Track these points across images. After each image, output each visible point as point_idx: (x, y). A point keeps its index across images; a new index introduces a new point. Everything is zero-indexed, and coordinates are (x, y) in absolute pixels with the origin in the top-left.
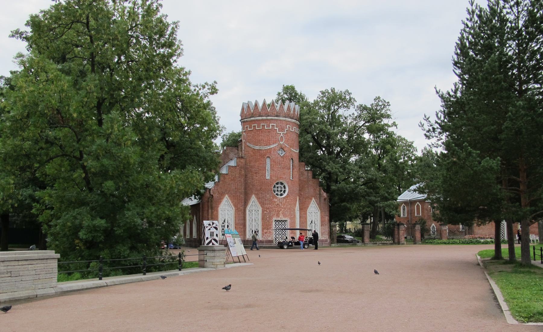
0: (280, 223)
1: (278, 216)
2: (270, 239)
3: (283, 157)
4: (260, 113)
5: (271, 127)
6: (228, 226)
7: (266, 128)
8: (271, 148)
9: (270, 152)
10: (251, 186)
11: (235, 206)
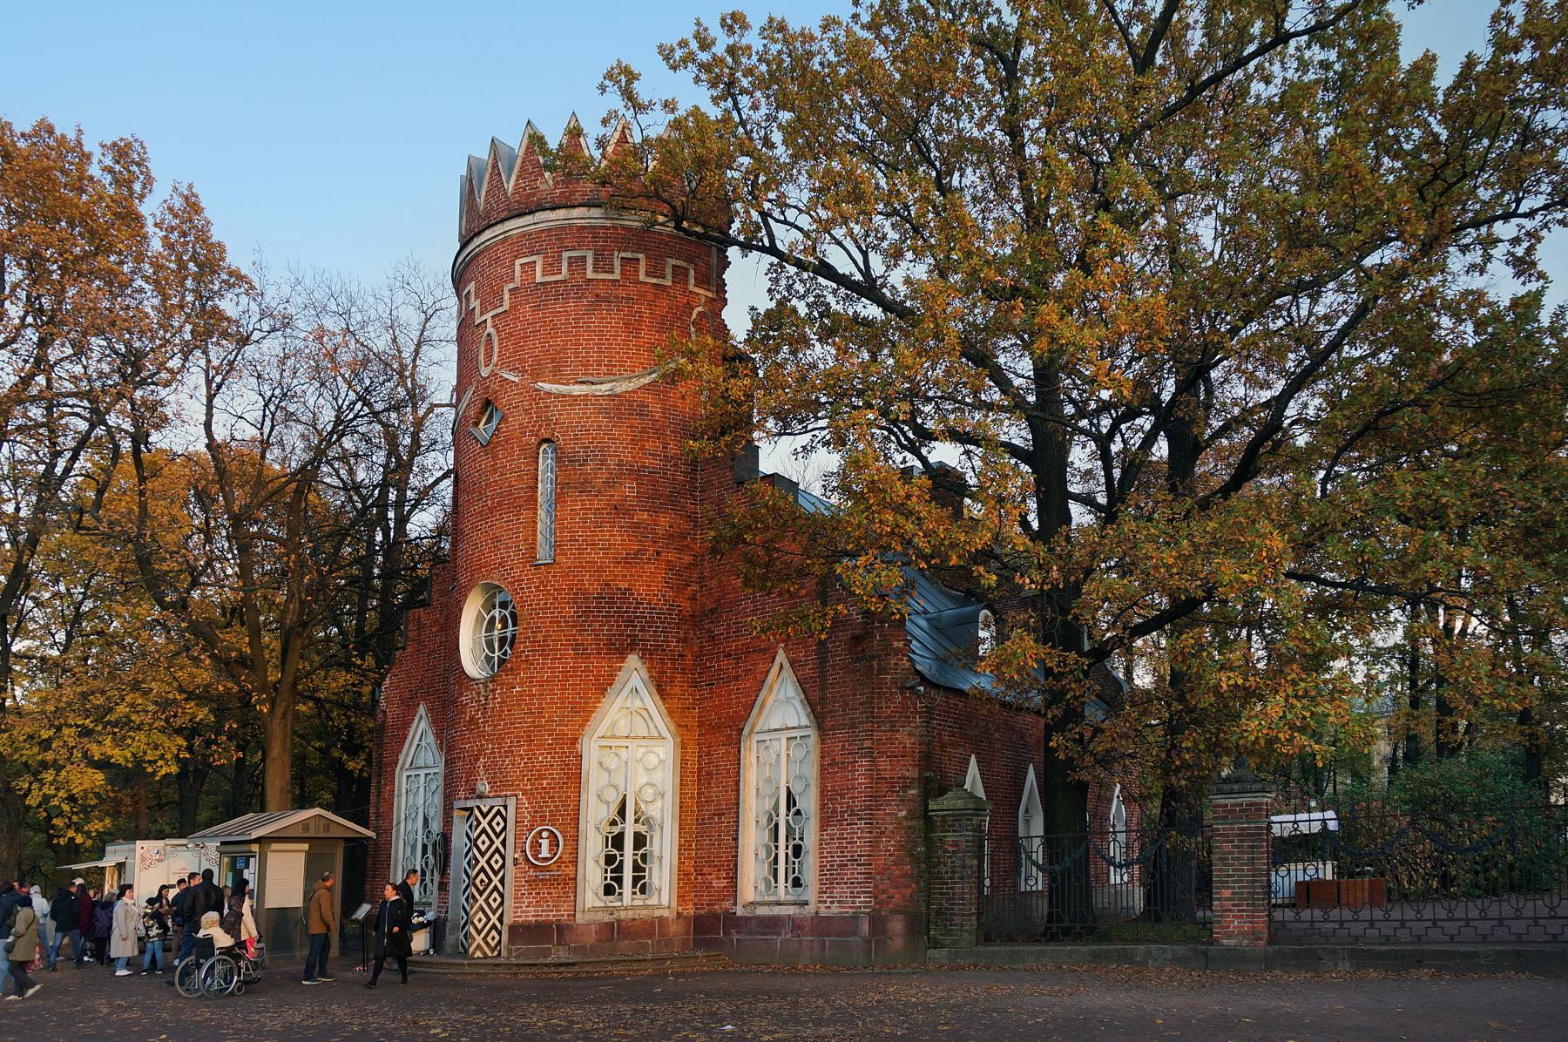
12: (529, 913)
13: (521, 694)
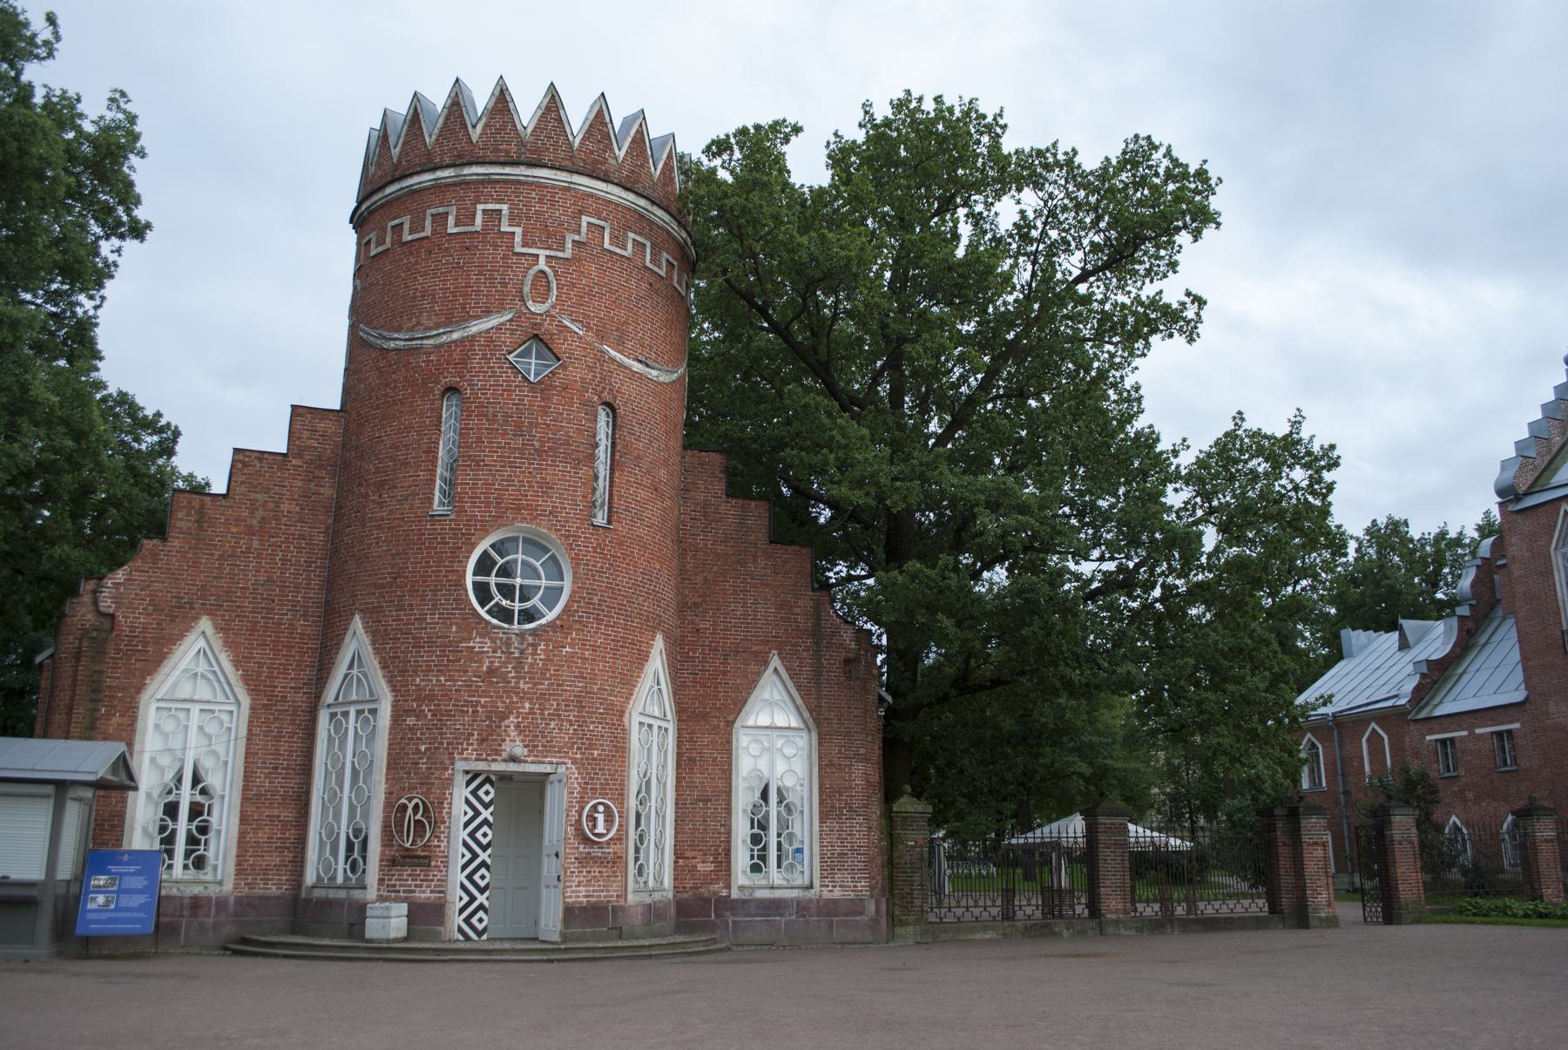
1: (490, 743)
3: (543, 388)
4: (429, 154)
5: (479, 219)
6: (196, 811)
8: (472, 339)
9: (464, 361)
11: (253, 683)
12: (580, 894)
13: (573, 655)
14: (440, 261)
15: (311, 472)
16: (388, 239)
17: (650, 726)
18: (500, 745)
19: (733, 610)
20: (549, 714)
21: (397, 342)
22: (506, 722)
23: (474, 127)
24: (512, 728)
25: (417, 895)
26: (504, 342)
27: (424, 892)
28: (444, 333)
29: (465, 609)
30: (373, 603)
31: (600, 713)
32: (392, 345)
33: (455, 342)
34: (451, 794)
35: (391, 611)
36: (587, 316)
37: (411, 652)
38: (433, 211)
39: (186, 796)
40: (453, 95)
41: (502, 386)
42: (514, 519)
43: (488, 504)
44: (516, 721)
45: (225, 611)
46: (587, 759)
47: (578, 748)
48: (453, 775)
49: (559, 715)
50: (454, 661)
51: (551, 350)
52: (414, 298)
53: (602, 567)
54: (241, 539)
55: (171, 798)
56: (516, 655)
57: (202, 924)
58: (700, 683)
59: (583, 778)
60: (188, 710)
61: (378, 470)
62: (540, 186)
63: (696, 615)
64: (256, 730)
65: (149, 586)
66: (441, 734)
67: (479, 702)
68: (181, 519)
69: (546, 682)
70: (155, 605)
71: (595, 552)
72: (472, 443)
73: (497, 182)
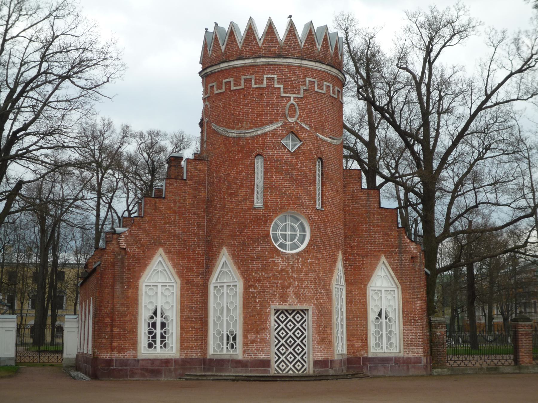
0: (290, 317)
1: (283, 298)
2: (262, 356)
5: (265, 82)
6: (163, 325)
7: (254, 86)
8: (266, 134)
9: (263, 144)
10: (219, 227)
12: (319, 357)
13: (312, 262)
14: (249, 99)
15: (197, 187)
16: (224, 87)
17: (338, 288)
18: (287, 299)
19: (366, 238)
20: (305, 286)
21: (233, 134)
22: (288, 290)
23: (260, 40)
24: (291, 292)
25: (259, 356)
26: (279, 135)
27: (262, 356)
28: (254, 131)
29: (270, 246)
30: (231, 243)
31: (322, 285)
32: (231, 135)
33: (259, 135)
34: (270, 318)
35: (240, 246)
36: (311, 122)
37: (250, 263)
38: (245, 77)
39: (159, 320)
40: (249, 25)
41: (280, 154)
42: (287, 209)
43: (277, 203)
44: (292, 289)
45: (168, 245)
46: (319, 303)
47: (315, 299)
48: (270, 311)
49: (308, 287)
50: (267, 266)
51: (297, 137)
52: (239, 115)
53: (321, 226)
54: (171, 215)
55: (153, 321)
56: (291, 263)
57: (170, 369)
58: (353, 269)
59: (318, 311)
60: (157, 286)
61: (228, 188)
62: (289, 66)
63: (351, 240)
64: (184, 293)
65: (138, 236)
66: (264, 295)
67: (278, 282)
68: (148, 209)
69: (303, 274)
70: (141, 244)
71: (318, 220)
72: (269, 177)
73: (272, 65)
